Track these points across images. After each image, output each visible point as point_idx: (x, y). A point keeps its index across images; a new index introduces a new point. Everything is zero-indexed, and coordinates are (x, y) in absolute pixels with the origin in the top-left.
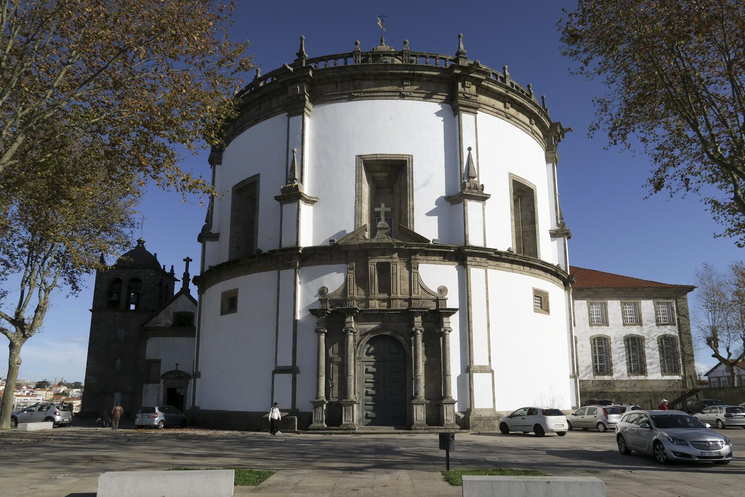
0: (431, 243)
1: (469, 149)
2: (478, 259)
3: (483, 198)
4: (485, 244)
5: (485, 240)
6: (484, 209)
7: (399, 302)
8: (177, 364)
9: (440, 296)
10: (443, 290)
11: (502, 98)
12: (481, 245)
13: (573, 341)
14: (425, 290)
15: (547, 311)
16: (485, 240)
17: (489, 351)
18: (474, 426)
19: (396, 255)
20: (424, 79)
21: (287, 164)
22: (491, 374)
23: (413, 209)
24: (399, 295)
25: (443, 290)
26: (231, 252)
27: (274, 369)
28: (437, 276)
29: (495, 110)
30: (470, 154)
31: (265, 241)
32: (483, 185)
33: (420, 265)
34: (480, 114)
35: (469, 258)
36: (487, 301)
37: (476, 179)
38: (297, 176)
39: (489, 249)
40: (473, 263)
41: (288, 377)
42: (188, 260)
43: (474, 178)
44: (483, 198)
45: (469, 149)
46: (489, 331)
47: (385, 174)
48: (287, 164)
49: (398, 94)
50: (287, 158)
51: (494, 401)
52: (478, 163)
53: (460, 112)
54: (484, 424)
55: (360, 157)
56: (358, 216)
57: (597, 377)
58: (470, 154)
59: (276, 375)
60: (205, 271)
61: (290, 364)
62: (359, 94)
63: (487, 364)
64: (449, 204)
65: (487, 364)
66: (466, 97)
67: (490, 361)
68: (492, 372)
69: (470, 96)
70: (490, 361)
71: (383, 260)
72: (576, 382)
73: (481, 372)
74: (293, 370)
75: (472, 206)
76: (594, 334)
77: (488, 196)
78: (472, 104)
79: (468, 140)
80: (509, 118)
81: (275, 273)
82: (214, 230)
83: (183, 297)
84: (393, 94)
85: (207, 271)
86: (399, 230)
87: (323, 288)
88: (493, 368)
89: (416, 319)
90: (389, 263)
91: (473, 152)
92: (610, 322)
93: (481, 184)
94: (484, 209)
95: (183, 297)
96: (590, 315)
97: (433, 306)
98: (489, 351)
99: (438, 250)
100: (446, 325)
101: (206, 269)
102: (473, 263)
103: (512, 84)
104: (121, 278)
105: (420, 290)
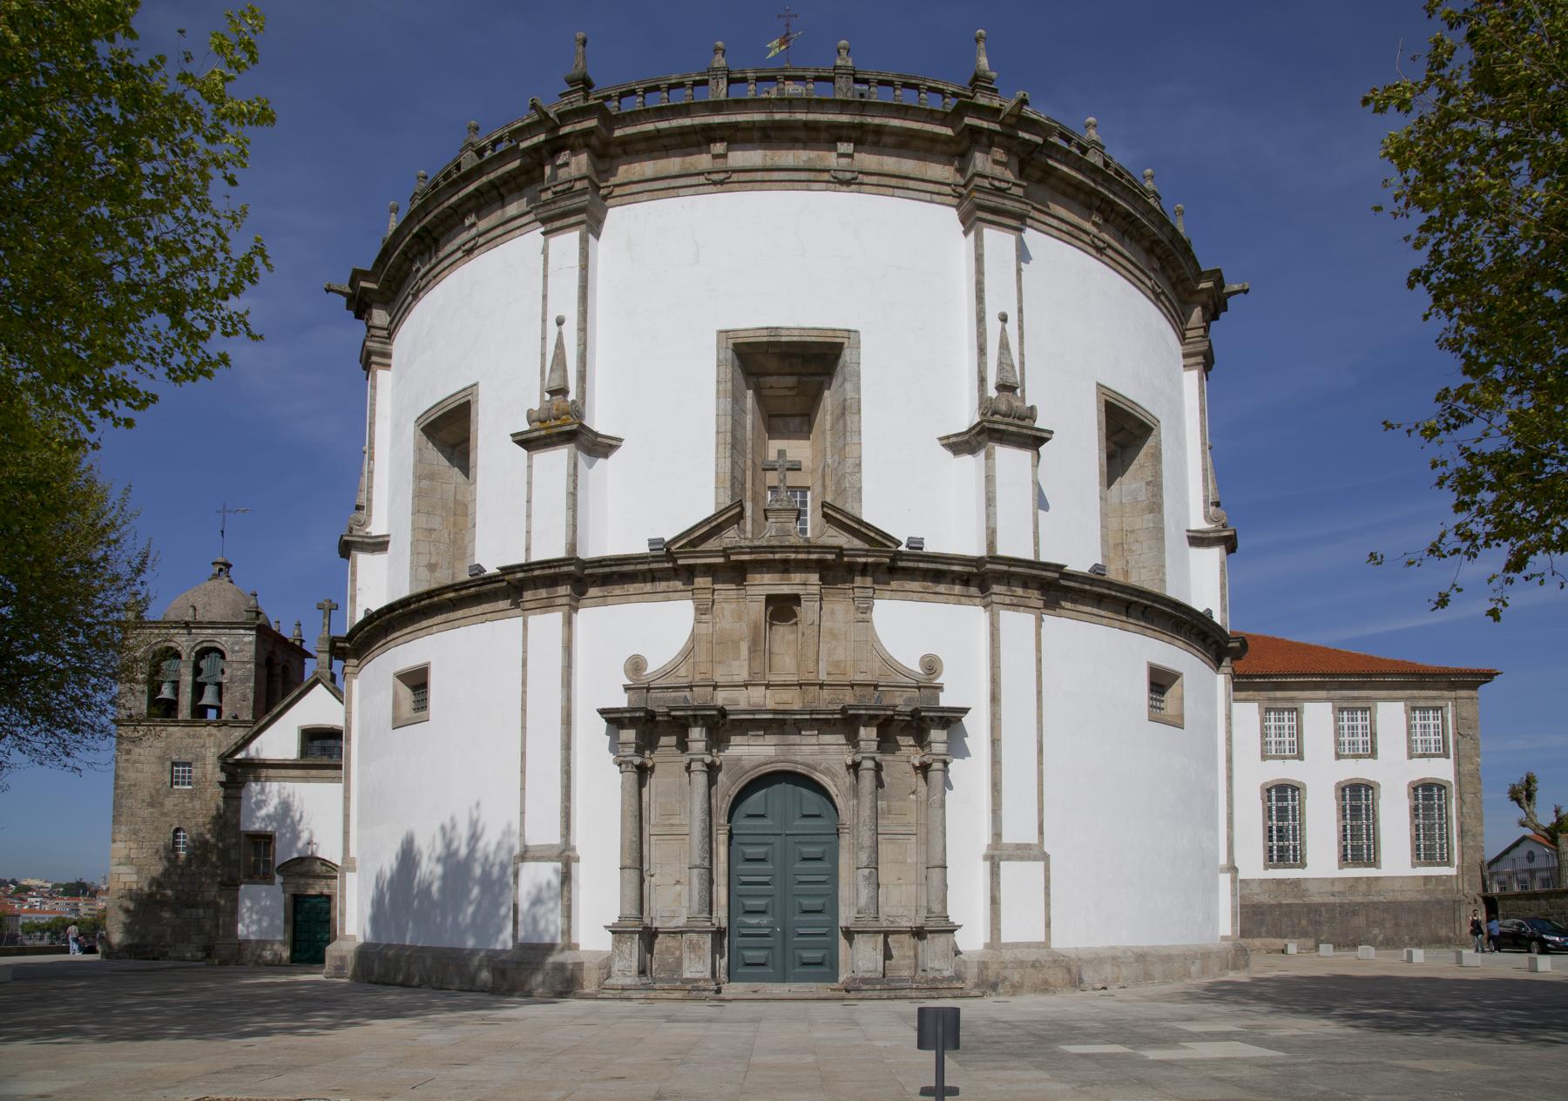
0: (903, 548)
3: (1034, 441)
4: (1037, 552)
5: (1036, 544)
7: (825, 694)
9: (924, 681)
10: (932, 665)
12: (1031, 557)
16: (1036, 544)
19: (814, 578)
20: (887, 139)
21: (543, 355)
23: (859, 465)
24: (823, 677)
25: (932, 665)
30: (1003, 329)
32: (1032, 408)
35: (996, 588)
36: (1039, 693)
39: (1046, 566)
40: (1007, 600)
44: (1034, 441)
47: (791, 381)
48: (543, 355)
49: (826, 176)
50: (544, 339)
51: (1048, 925)
52: (1022, 355)
58: (1003, 329)
61: (556, 839)
64: (949, 454)
66: (998, 189)
67: (1041, 832)
69: (1004, 185)
70: (1041, 832)
71: (786, 590)
75: (1009, 458)
77: (1045, 435)
78: (1009, 205)
79: (1000, 298)
84: (812, 176)
86: (825, 515)
88: (1047, 849)
89: (862, 730)
90: (796, 599)
93: (1028, 404)
99: (921, 565)
100: (939, 748)
102: (1007, 600)
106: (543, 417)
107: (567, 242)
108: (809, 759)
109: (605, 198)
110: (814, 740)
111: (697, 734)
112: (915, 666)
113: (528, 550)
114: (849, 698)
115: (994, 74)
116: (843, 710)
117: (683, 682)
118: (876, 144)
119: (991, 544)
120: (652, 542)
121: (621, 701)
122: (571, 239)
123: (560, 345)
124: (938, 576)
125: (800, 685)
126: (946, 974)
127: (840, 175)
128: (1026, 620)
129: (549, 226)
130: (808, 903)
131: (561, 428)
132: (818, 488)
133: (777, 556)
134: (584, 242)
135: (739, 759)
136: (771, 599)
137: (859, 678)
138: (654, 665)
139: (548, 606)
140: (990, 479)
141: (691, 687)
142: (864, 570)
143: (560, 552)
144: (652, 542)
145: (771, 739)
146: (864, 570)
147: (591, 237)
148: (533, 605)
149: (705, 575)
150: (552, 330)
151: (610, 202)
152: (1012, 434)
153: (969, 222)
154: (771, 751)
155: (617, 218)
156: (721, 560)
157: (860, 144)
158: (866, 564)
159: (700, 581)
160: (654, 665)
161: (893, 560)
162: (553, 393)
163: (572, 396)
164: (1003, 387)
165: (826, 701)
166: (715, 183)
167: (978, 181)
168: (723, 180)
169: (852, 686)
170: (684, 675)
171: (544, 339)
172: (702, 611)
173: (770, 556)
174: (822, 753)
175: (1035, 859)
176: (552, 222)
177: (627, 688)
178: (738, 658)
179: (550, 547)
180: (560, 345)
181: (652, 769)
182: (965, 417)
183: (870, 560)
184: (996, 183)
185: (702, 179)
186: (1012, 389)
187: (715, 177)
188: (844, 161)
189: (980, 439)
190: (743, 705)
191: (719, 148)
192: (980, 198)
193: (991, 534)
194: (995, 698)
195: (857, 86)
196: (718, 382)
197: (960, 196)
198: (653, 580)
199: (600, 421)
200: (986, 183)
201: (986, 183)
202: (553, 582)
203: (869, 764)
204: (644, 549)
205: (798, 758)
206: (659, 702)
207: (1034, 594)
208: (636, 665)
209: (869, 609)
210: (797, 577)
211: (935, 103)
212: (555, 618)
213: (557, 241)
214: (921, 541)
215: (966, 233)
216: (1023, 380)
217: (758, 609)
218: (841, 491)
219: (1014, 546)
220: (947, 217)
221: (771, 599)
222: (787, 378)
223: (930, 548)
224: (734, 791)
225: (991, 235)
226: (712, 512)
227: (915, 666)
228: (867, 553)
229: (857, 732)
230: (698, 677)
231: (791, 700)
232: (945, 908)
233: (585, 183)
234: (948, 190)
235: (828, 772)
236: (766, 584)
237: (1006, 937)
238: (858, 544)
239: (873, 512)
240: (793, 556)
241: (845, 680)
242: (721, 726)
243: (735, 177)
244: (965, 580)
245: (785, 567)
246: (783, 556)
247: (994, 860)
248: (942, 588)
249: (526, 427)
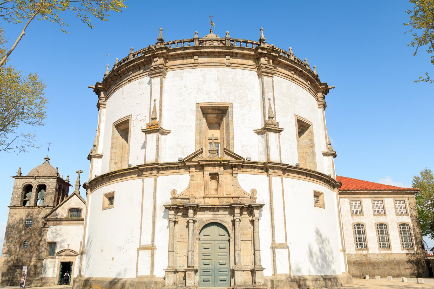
1: (269, 100)
2: (277, 171)
4: (281, 160)
5: (281, 158)
6: (279, 138)
7: (225, 200)
8: (69, 245)
9: (252, 196)
10: (254, 192)
11: (289, 67)
12: (278, 161)
13: (341, 226)
14: (242, 191)
15: (323, 206)
17: (286, 234)
18: (277, 286)
19: (222, 168)
21: (150, 109)
22: (286, 250)
23: (233, 138)
24: (225, 195)
25: (254, 192)
26: (110, 167)
27: (138, 247)
28: (249, 183)
29: (284, 75)
32: (278, 123)
33: (238, 175)
34: (275, 78)
35: (270, 170)
36: (283, 199)
37: (274, 119)
40: (274, 174)
41: (149, 252)
42: (80, 173)
43: (272, 118)
44: (279, 131)
45: (269, 100)
46: (285, 219)
48: (150, 109)
49: (223, 64)
50: (150, 104)
52: (275, 109)
53: (263, 76)
54: (284, 285)
57: (358, 251)
58: (270, 102)
59: (141, 252)
60: (92, 179)
62: (197, 64)
63: (284, 242)
64: (256, 135)
65: (284, 242)
67: (286, 240)
68: (288, 248)
70: (286, 240)
72: (344, 255)
73: (281, 248)
74: (152, 249)
75: (272, 136)
76: (354, 222)
78: (270, 71)
79: (269, 95)
80: (294, 80)
82: (99, 151)
85: (94, 180)
86: (225, 152)
87: (174, 190)
88: (288, 245)
90: (217, 174)
91: (272, 101)
92: (365, 213)
94: (279, 138)
96: (351, 208)
97: (247, 202)
98: (286, 234)
100: (256, 215)
101: (93, 178)
102: (274, 174)
103: (295, 59)
104: (32, 184)
105: (239, 192)
106: (150, 125)
107: (156, 81)
108: (221, 219)
109: (167, 69)
110: (222, 213)
111: (191, 212)
112: (249, 192)
113: (145, 160)
114: (231, 201)
115: (265, 39)
116: (230, 205)
117: (187, 197)
118: (236, 56)
119: (268, 159)
120: (179, 159)
121: (170, 202)
122: (159, 79)
123: (155, 106)
124: (254, 167)
125: (218, 198)
126: (262, 284)
127: (227, 64)
129: (152, 76)
130: (221, 261)
132: (222, 143)
133: (212, 163)
134: (161, 80)
135: (202, 219)
136: (210, 174)
137: (234, 196)
138: (179, 192)
139: (150, 176)
140: (267, 141)
141: (189, 199)
142: (235, 166)
143: (154, 161)
144: (179, 159)
145: (211, 213)
146: (235, 166)
147: (163, 79)
148: (146, 175)
149: (193, 167)
150: (153, 103)
151: (168, 70)
152: (273, 130)
153: (260, 76)
154: (211, 216)
155: (170, 74)
156: (197, 164)
157: (232, 56)
158: (236, 165)
159: (192, 169)
160: (179, 192)
161: (243, 163)
162: (152, 119)
163: (158, 120)
164: (270, 118)
165: (225, 202)
166: (195, 66)
167: (262, 65)
168: (196, 65)
169: (232, 198)
170: (187, 195)
171: (150, 104)
172: (192, 177)
173: (211, 163)
174: (225, 217)
175: (285, 248)
176: (152, 75)
177: (171, 199)
178: (202, 190)
179: (151, 159)
180: (155, 106)
181: (178, 222)
182: (260, 125)
183: (237, 163)
184: (267, 66)
185: (192, 65)
186: (272, 118)
187: (195, 65)
188: (228, 61)
189: (265, 131)
190: (203, 204)
191: (196, 57)
192: (262, 70)
193: (268, 156)
194: (271, 201)
195: (231, 42)
196: (196, 116)
197: (258, 69)
198: (179, 169)
199: (165, 126)
200: (264, 66)
201: (264, 66)
202: (152, 169)
203: (238, 220)
204: (176, 161)
205: (218, 218)
206: (179, 203)
207: (281, 172)
208: (174, 192)
209: (237, 176)
210: (217, 168)
211: (250, 46)
212: (152, 179)
213: (154, 80)
214: (250, 158)
215: (259, 78)
216: (275, 116)
217: (207, 177)
218: (228, 145)
219: (275, 158)
220: (254, 74)
221: (210, 174)
222: (216, 115)
223: (252, 160)
224: (201, 228)
225: (266, 79)
226: (194, 151)
227: (249, 192)
228: (236, 162)
229: (234, 211)
230: (191, 196)
231: (216, 202)
232: (260, 263)
233: (162, 66)
234: (254, 67)
235: (226, 222)
236: (209, 170)
237: (279, 272)
238: (233, 159)
239: (238, 150)
240: (216, 163)
241: (231, 196)
242: (197, 209)
243: (200, 65)
244: (262, 168)
245: (214, 166)
246: (214, 163)
247: (273, 248)
248: (256, 170)
249: (145, 128)
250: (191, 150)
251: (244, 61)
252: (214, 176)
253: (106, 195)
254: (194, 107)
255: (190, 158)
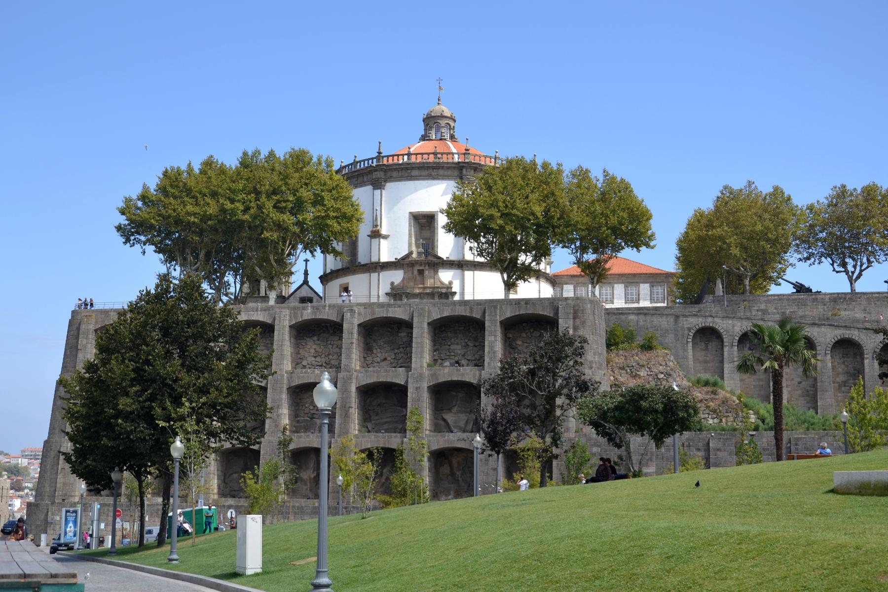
14: (441, 283)
25: (451, 283)
31: (362, 259)
38: (379, 223)
55: (410, 213)
56: (410, 245)
81: (367, 275)
83: (305, 286)
95: (305, 286)
97: (444, 291)
101: (328, 271)
107: (377, 192)
128: (471, 273)
131: (376, 234)
139: (375, 272)
172: (405, 273)
193: (464, 255)
208: (392, 284)
217: (416, 272)
245: (421, 265)
250: (404, 252)
251: (449, 172)
252: (421, 272)
253: (341, 285)
254: (407, 215)
255: (403, 258)
